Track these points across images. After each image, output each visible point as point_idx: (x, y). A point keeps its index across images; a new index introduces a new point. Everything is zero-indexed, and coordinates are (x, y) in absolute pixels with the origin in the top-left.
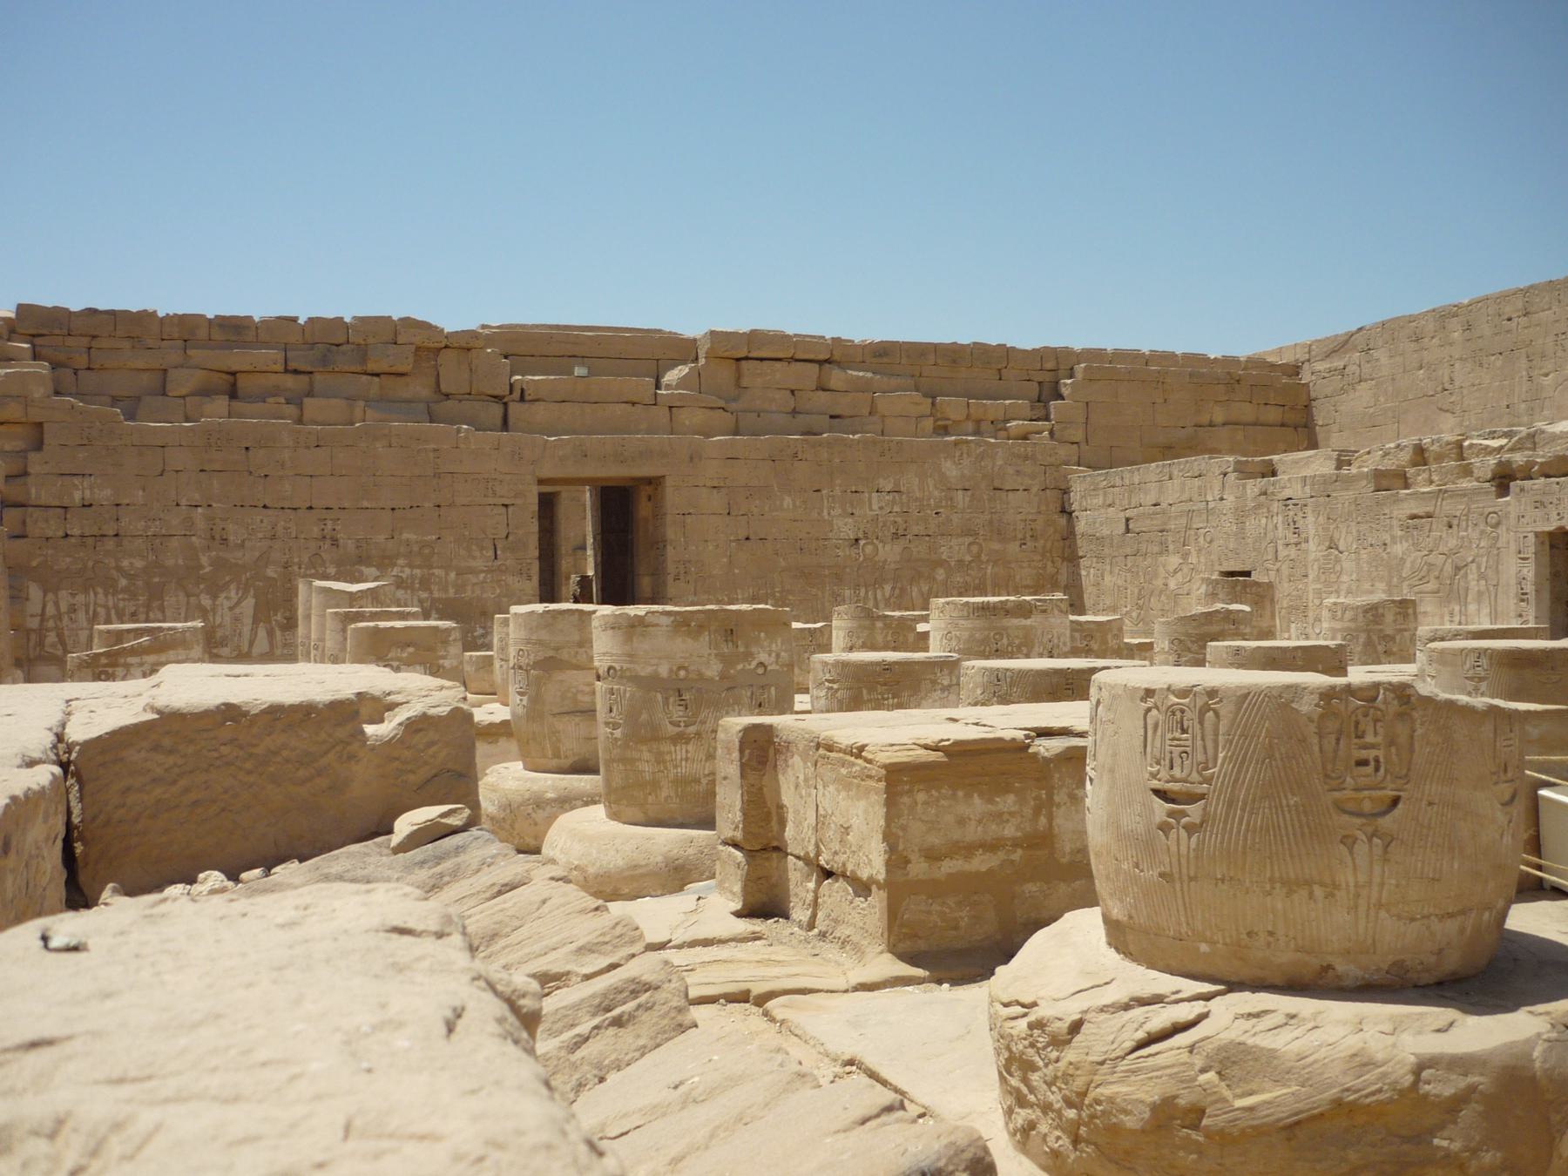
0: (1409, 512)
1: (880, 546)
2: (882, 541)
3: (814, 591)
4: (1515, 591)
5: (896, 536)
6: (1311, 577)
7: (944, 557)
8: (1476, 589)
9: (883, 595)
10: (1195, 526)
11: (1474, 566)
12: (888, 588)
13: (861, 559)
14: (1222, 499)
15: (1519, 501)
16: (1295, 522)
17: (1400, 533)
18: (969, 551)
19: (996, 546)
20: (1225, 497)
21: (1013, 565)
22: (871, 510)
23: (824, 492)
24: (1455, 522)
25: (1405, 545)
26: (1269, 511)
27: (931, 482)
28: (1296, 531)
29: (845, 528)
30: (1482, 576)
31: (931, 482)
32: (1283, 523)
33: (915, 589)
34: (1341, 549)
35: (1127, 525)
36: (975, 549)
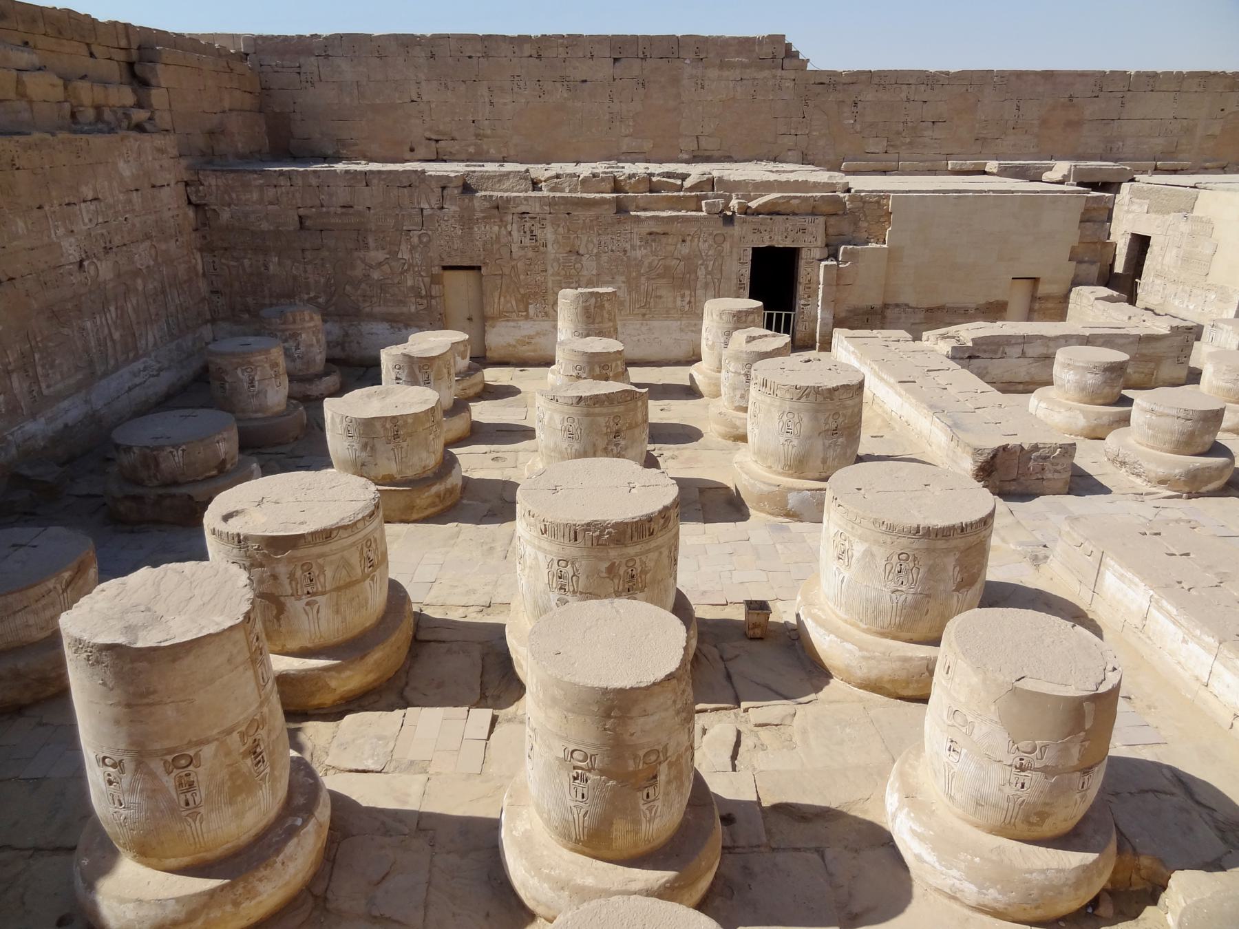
0: (648, 230)
1: (99, 265)
2: (99, 259)
3: (66, 331)
4: (735, 281)
5: (107, 250)
6: (550, 271)
7: (139, 266)
8: (704, 280)
9: (112, 318)
10: (405, 228)
11: (703, 267)
12: (112, 309)
13: (89, 283)
14: (442, 208)
15: (742, 228)
16: (532, 231)
17: (638, 243)
18: (151, 256)
19: (163, 247)
20: (445, 206)
21: (175, 263)
22: (85, 224)
23: (47, 208)
24: (689, 238)
25: (644, 252)
26: (501, 221)
27: (115, 184)
28: (533, 237)
29: (70, 248)
30: (708, 273)
31: (115, 184)
32: (519, 231)
33: (129, 306)
34: (581, 252)
35: (301, 223)
36: (153, 252)
